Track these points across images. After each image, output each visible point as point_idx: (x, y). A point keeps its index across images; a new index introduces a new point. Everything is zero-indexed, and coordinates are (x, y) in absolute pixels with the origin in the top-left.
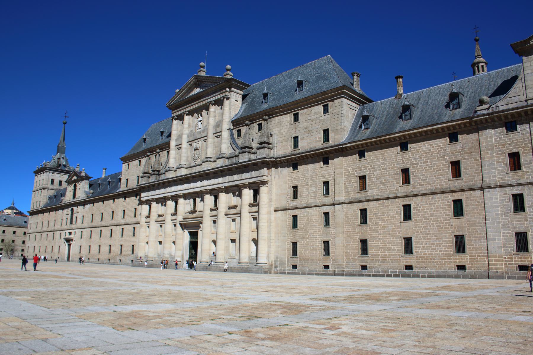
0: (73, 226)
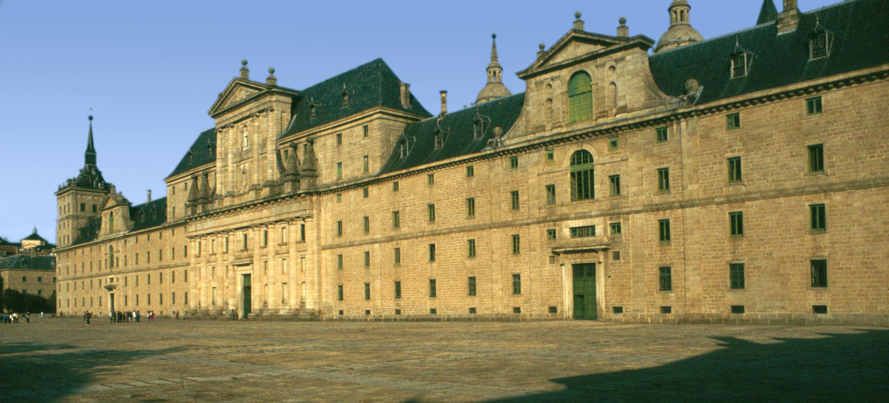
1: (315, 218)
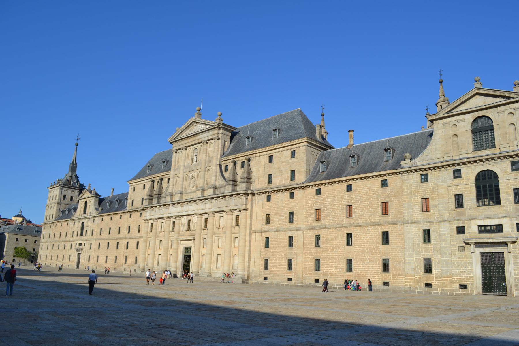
0: (84, 237)
1: (249, 212)
